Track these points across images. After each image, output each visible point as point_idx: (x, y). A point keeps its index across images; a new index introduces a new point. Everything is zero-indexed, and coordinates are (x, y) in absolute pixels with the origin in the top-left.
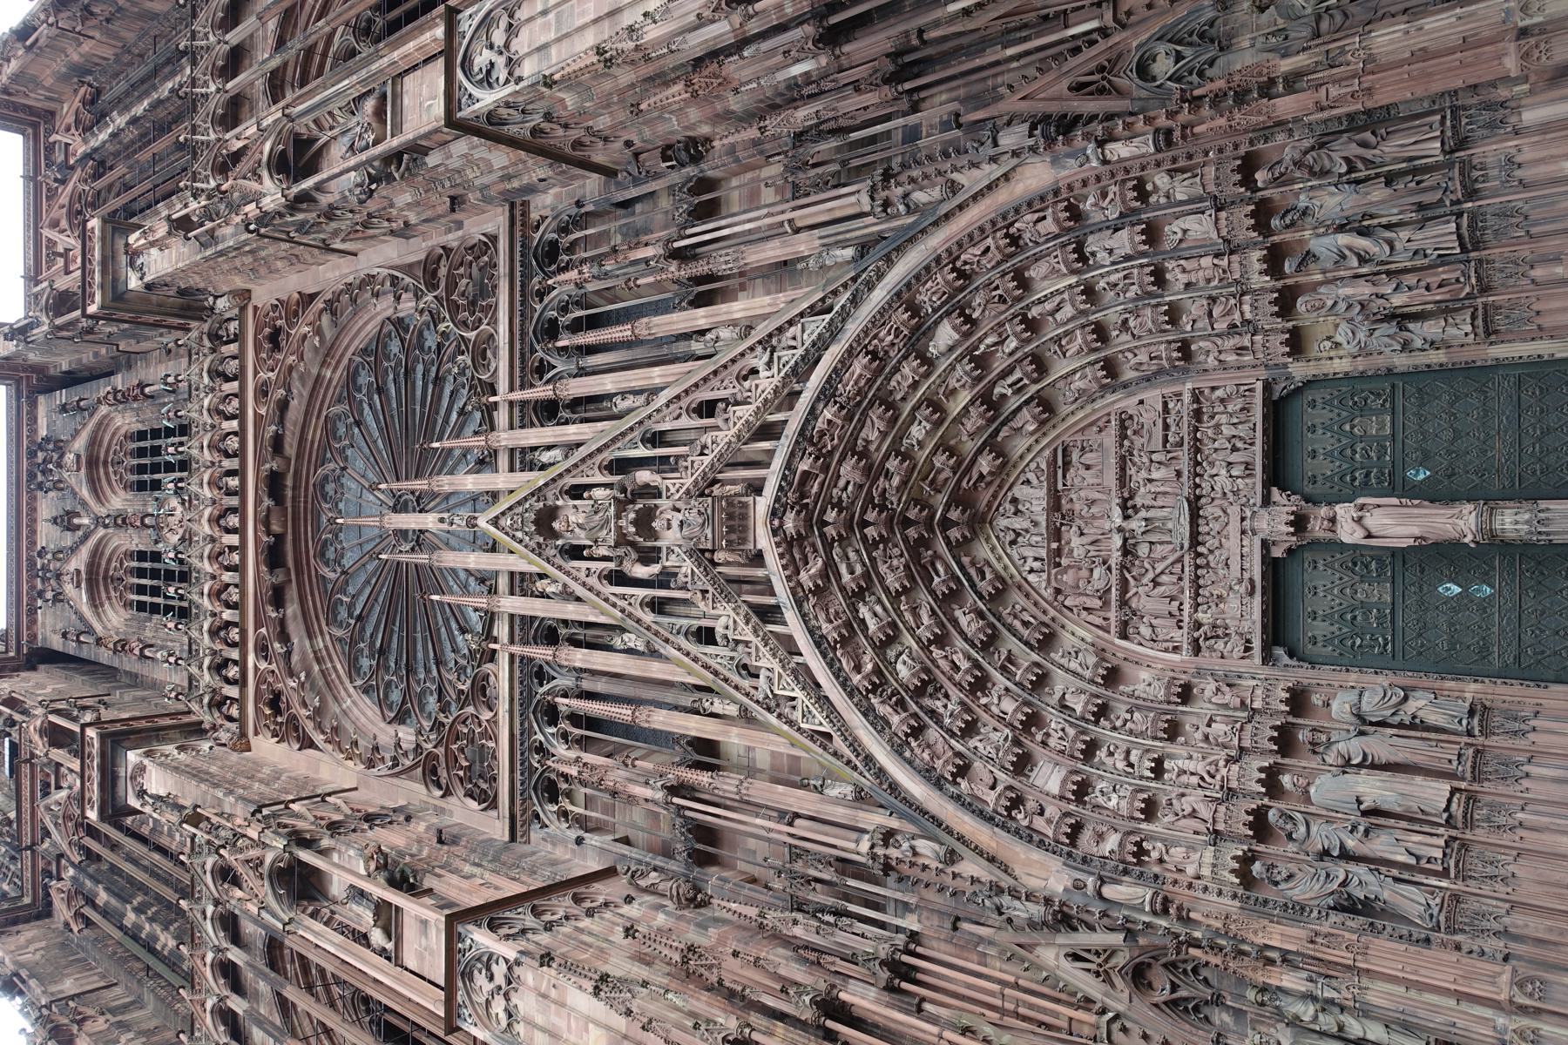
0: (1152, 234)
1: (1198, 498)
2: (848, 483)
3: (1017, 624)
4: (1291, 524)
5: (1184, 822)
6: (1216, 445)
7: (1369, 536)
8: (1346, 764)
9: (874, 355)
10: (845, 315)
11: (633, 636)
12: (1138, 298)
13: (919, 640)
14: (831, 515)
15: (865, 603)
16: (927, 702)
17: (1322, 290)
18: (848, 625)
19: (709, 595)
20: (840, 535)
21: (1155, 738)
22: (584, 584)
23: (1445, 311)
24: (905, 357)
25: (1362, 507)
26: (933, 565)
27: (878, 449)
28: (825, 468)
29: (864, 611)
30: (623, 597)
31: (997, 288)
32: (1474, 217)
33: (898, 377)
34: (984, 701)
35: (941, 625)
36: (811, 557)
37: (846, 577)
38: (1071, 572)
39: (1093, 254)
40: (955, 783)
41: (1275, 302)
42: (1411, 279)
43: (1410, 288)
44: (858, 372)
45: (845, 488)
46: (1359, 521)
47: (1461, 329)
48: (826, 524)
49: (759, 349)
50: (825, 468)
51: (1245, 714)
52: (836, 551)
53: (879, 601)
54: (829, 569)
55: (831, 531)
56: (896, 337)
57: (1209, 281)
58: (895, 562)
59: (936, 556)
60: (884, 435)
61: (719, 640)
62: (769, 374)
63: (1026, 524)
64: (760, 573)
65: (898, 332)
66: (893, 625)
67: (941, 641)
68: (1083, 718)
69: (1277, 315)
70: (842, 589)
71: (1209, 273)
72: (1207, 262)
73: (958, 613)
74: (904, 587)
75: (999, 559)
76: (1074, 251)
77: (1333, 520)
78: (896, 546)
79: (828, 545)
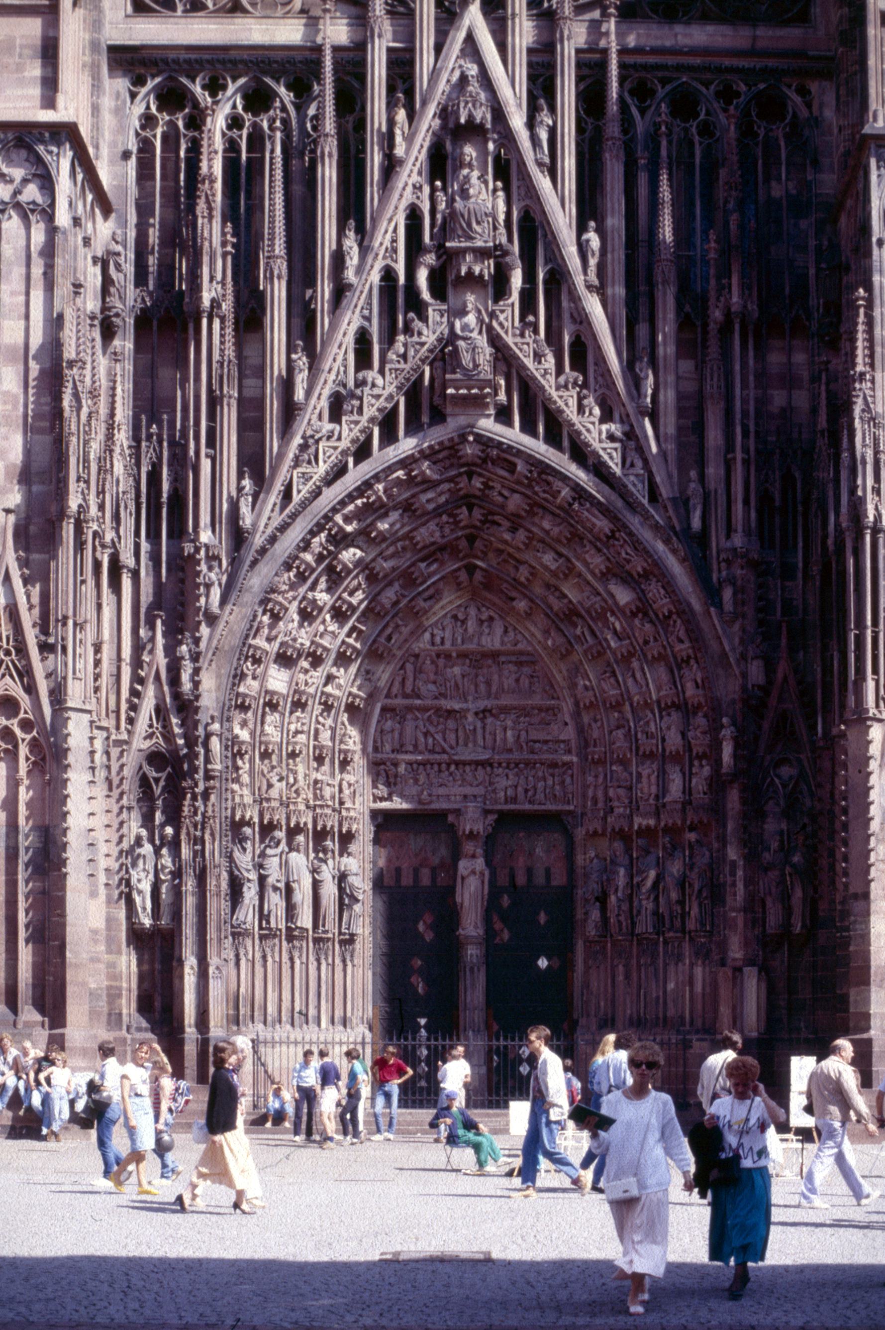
0: (676, 758)
1: (491, 765)
2: (506, 498)
3: (389, 630)
4: (471, 832)
5: (265, 782)
6: (531, 778)
7: (463, 878)
8: (314, 871)
9: (612, 536)
10: (646, 516)
11: (356, 260)
12: (637, 740)
13: (373, 560)
14: (477, 483)
15: (401, 515)
16: (323, 579)
17: (627, 857)
18: (383, 505)
19: (402, 366)
20: (460, 489)
21: (315, 747)
22: (406, 184)
23: (605, 919)
24: (608, 559)
25: (482, 874)
26: (436, 560)
27: (534, 524)
28: (519, 482)
29: (394, 516)
30: (394, 241)
31: (655, 638)
32: (657, 943)
33: (593, 551)
34: (328, 617)
35: (385, 576)
36: (439, 466)
37: (424, 498)
38: (433, 667)
39: (669, 715)
40: (264, 613)
41: (622, 830)
42: (625, 907)
43: (619, 907)
44: (598, 523)
45: (501, 494)
46: (473, 872)
47: (591, 931)
48: (470, 479)
49: (627, 428)
50: (519, 482)
51: (337, 806)
52: (446, 486)
53: (403, 526)
54: (428, 484)
55: (463, 482)
56: (625, 559)
57: (641, 790)
58: (438, 534)
59: (442, 563)
60: (547, 532)
61: (360, 375)
62: (604, 436)
63: (470, 630)
64: (425, 419)
65: (628, 561)
66: (384, 539)
67: (372, 578)
68: (323, 693)
69: (613, 829)
70: (413, 496)
71: (646, 790)
72: (654, 789)
73: (396, 586)
74: (417, 543)
75: (442, 608)
76: (673, 702)
77: (473, 856)
78: (452, 530)
79: (450, 480)
